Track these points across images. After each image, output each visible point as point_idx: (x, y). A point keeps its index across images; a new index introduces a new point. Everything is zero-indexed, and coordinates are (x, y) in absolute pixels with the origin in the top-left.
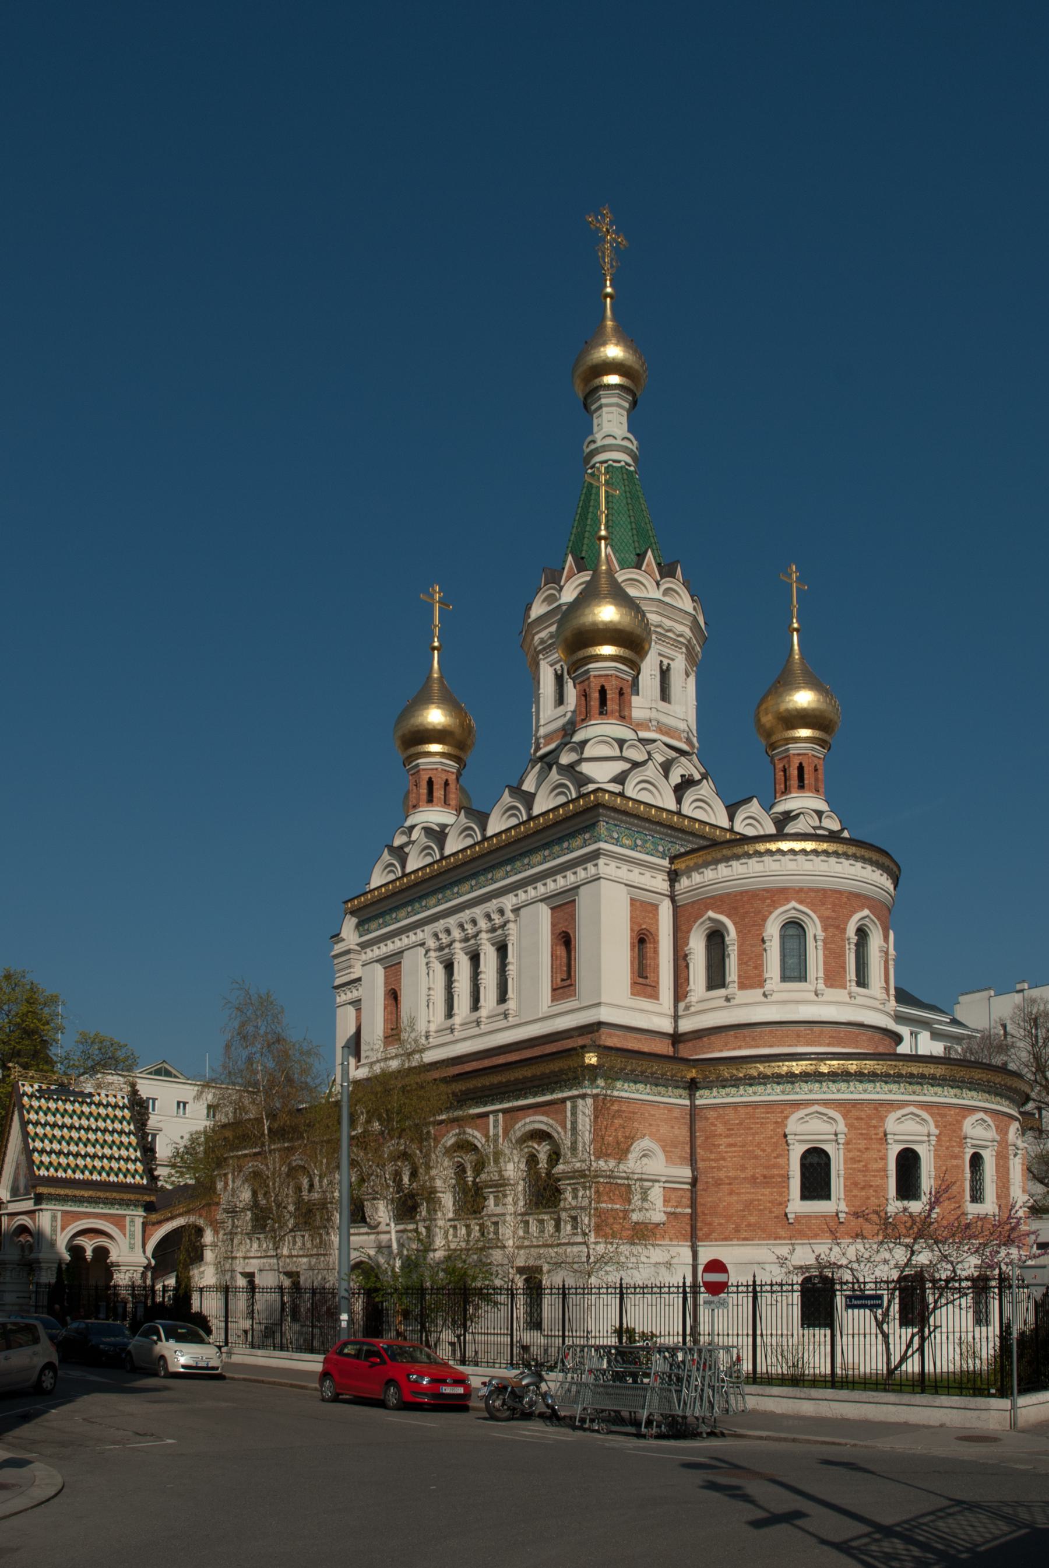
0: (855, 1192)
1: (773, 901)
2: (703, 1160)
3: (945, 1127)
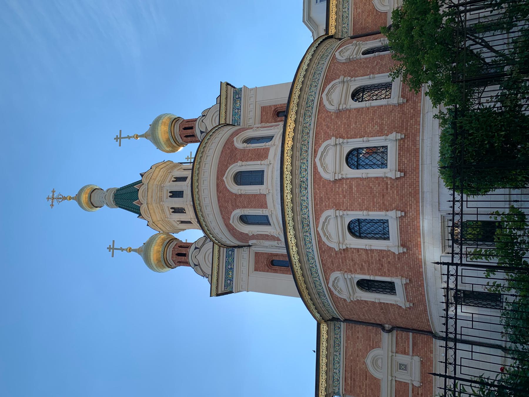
0: (385, 270)
3: (329, 199)
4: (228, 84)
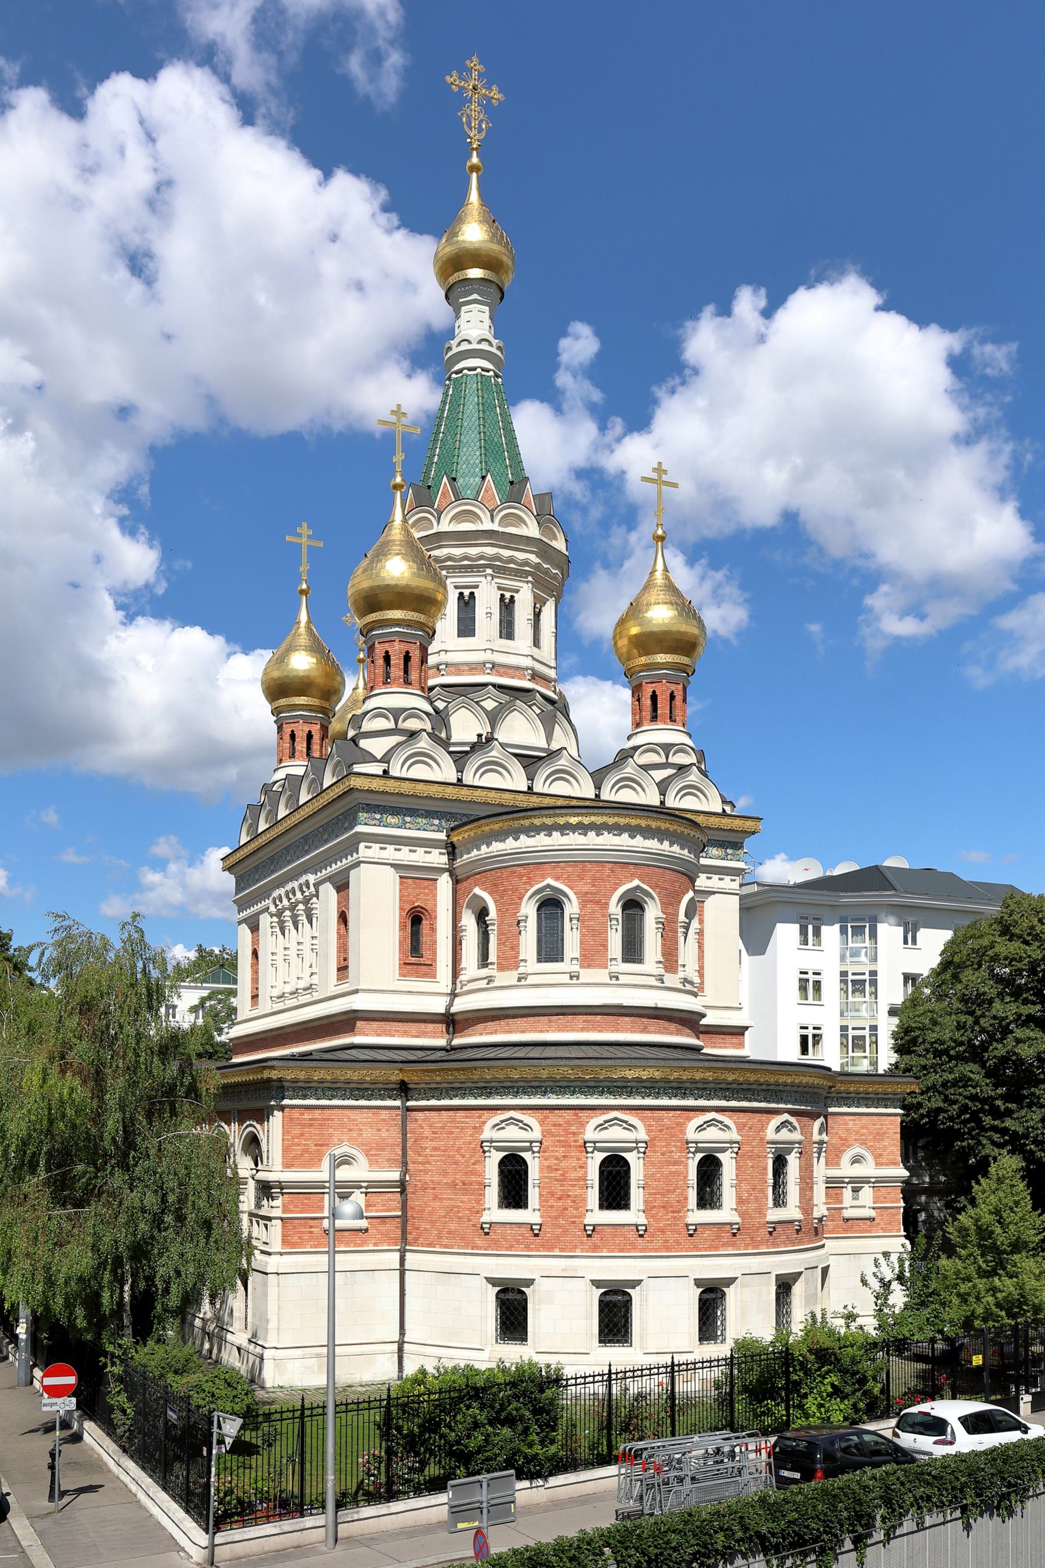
0: (552, 1202)
1: (529, 878)
2: (414, 1163)
3: (660, 1131)
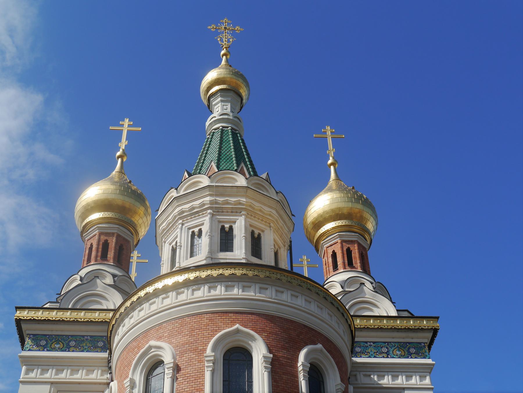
4: (435, 331)
